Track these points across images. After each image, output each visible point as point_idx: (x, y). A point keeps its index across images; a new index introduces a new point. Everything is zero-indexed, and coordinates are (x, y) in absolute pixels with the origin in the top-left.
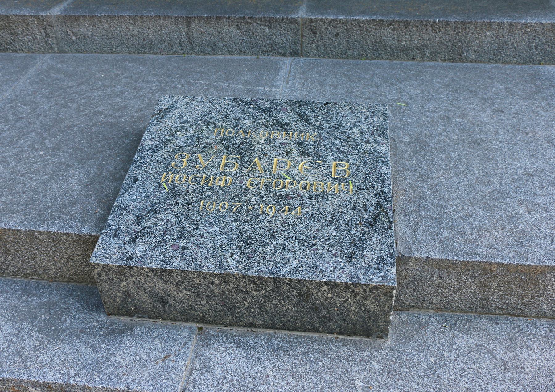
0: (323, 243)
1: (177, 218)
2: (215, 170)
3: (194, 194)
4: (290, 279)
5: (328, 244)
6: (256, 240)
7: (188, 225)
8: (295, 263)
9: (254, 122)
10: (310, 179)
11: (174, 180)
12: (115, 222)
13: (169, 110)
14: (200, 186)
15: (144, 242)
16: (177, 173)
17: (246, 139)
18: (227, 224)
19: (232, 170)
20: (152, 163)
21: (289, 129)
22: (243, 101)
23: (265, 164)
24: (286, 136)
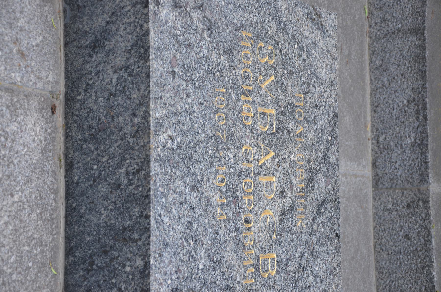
0: (190, 253)
1: (204, 59)
3: (231, 77)
4: (150, 216)
5: (189, 259)
6: (188, 166)
7: (198, 75)
8: (167, 220)
9: (313, 144)
10: (256, 227)
13: (321, 27)
14: (241, 84)
17: (294, 136)
18: (202, 126)
19: (259, 123)
20: (262, 14)
21: (307, 191)
22: (335, 126)
23: (269, 166)
24: (299, 188)
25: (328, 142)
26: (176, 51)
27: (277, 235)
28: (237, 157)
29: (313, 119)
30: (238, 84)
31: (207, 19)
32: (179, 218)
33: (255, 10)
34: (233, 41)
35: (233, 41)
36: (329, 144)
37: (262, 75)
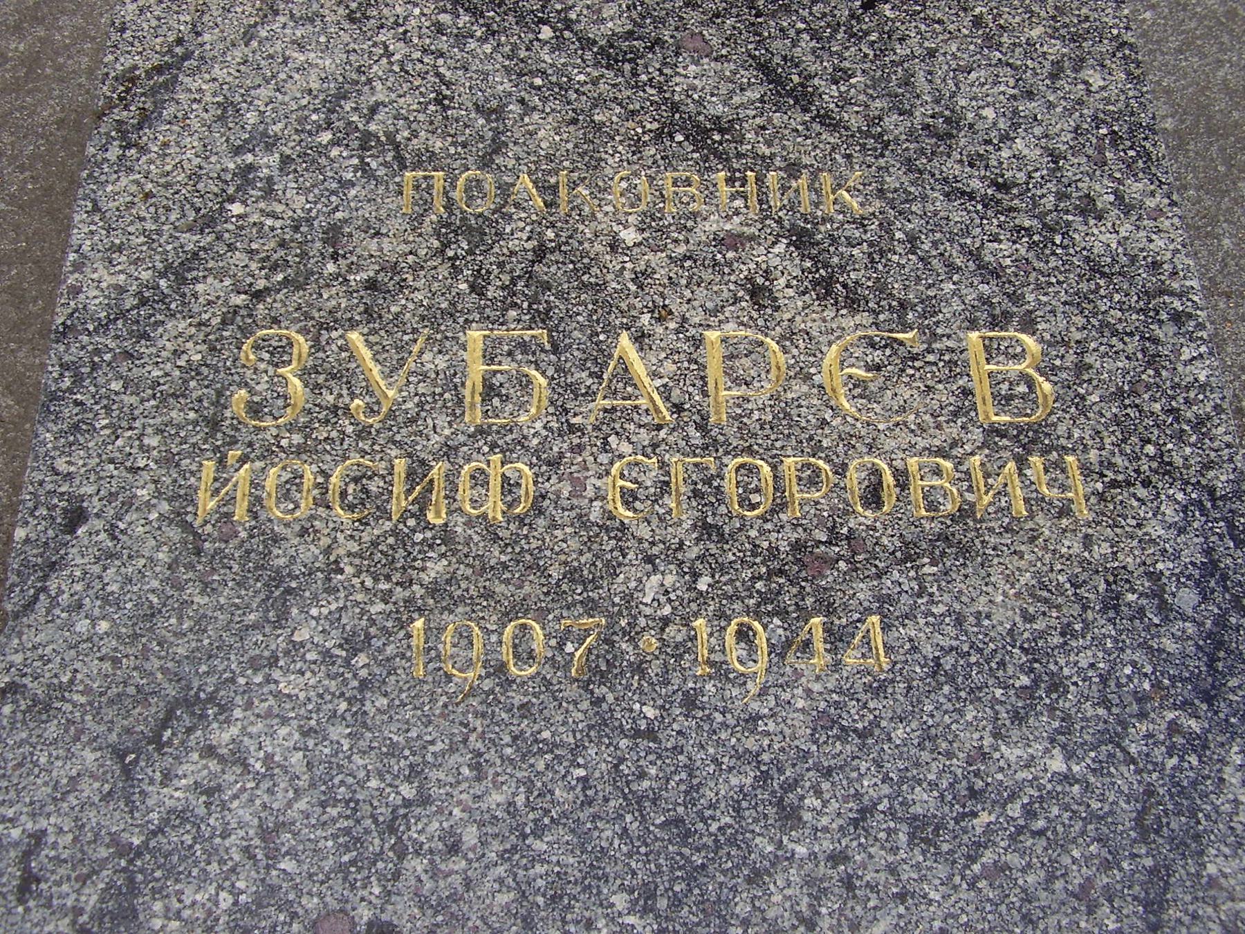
1: (311, 743)
2: (442, 420)
3: (369, 583)
5: (1041, 833)
6: (710, 843)
7: (374, 783)
9: (574, 121)
10: (890, 444)
11: (259, 500)
12: (13, 794)
15: (178, 915)
16: (268, 453)
20: (133, 400)
21: (739, 156)
24: (733, 197)
25: (558, 44)
26: (294, 915)
27: (906, 327)
28: (655, 550)
29: (488, 121)
30: (391, 540)
31: (164, 725)
32: (902, 897)
33: (119, 442)
34: (236, 568)
35: (236, 568)
36: (567, 34)
37: (347, 400)
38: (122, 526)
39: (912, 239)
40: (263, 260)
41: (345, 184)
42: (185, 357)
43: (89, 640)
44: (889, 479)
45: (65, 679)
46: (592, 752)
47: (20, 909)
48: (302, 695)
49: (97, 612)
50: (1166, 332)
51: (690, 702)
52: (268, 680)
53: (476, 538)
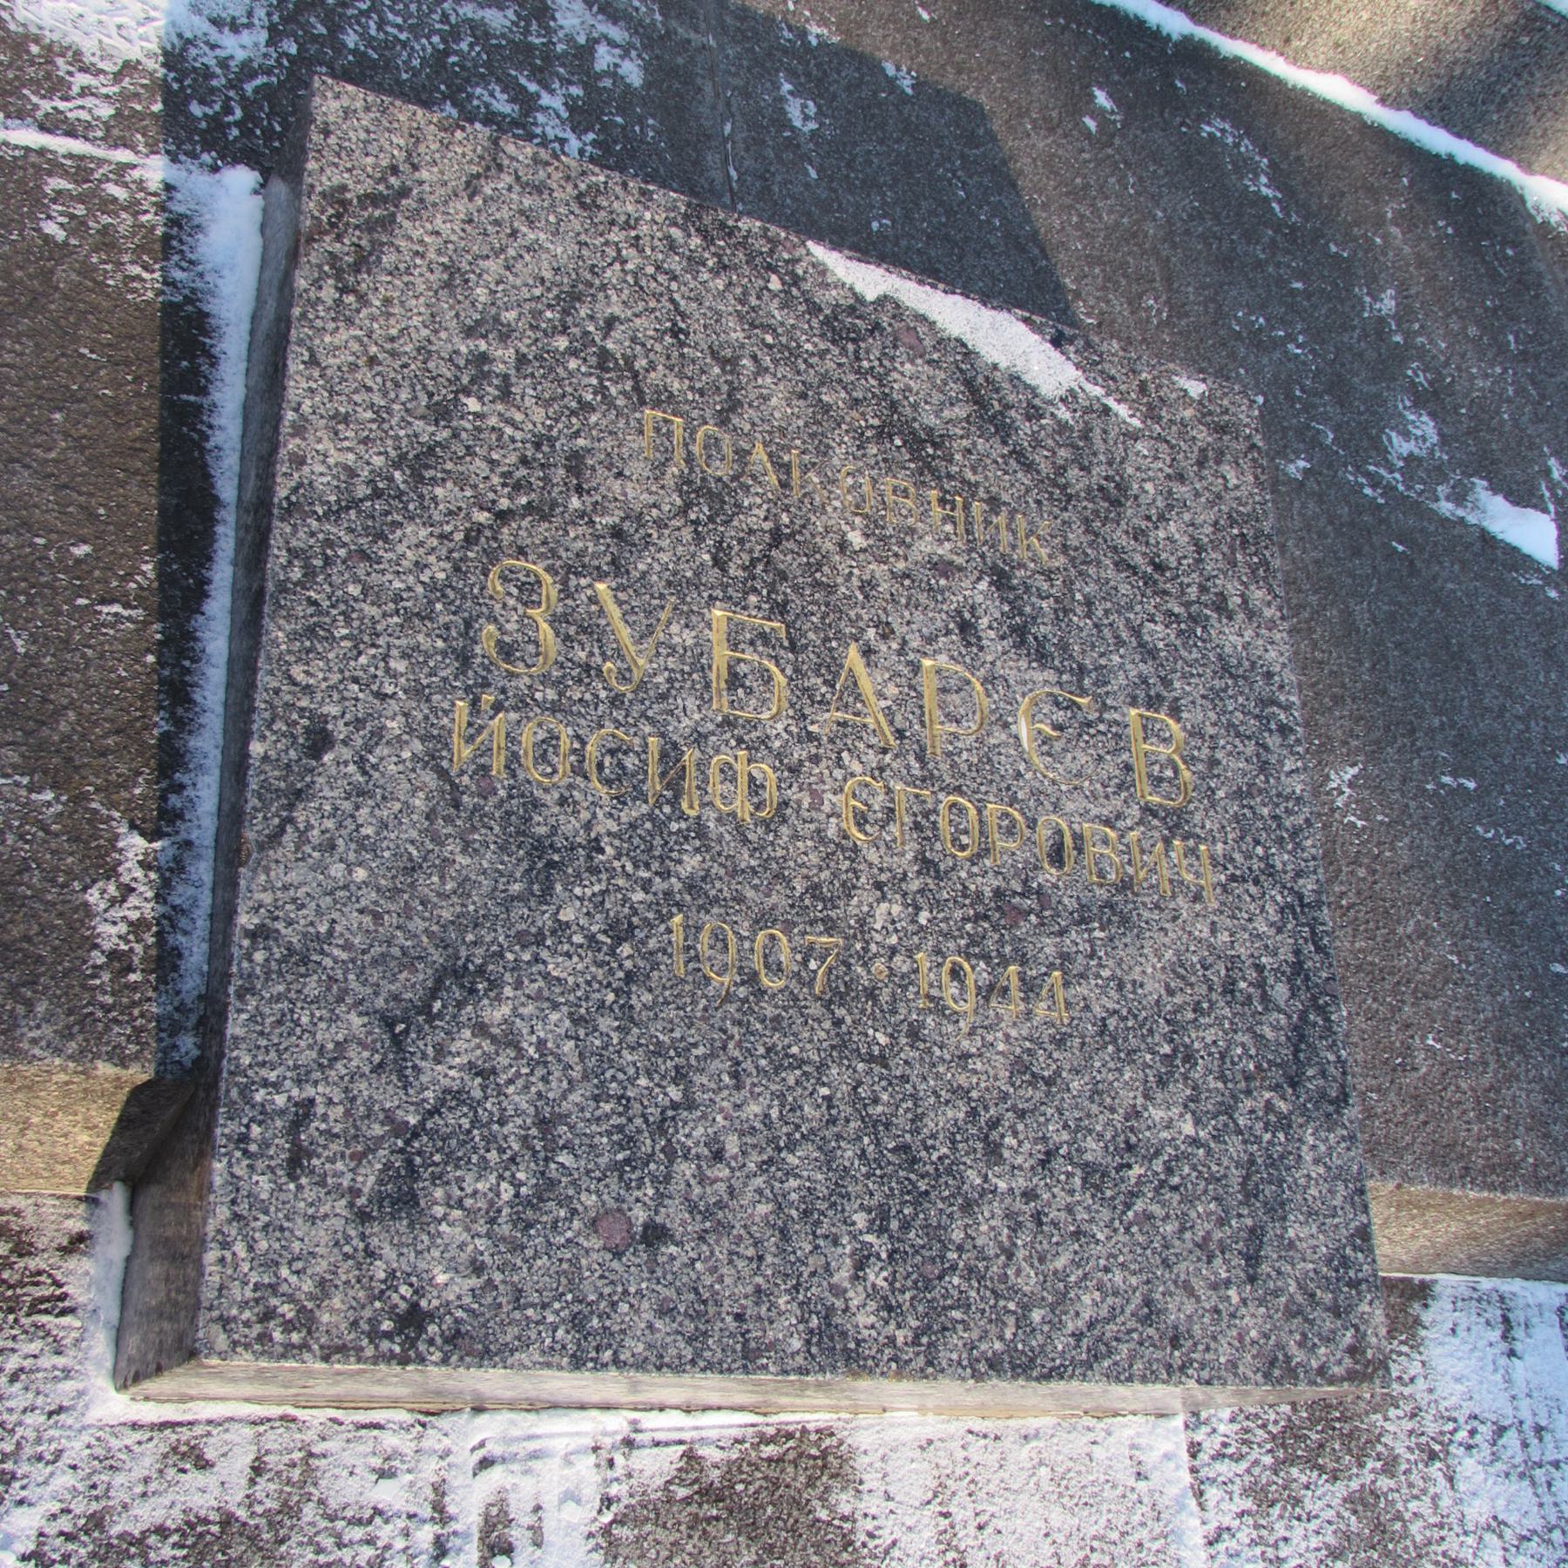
2: (691, 703)
3: (629, 868)
5: (1175, 1188)
7: (643, 1082)
9: (803, 396)
11: (515, 755)
12: (273, 1055)
15: (460, 1204)
20: (374, 611)
21: (950, 477)
26: (574, 1212)
27: (1083, 692)
28: (883, 877)
30: (648, 825)
31: (434, 994)
32: (1077, 1234)
33: (363, 660)
35: (497, 829)
36: (795, 291)
37: (599, 660)
38: (373, 760)
39: (1089, 603)
40: (504, 475)
41: (586, 407)
42: (428, 573)
43: (345, 887)
44: (1068, 841)
45: (323, 929)
46: (834, 1071)
47: (292, 1186)
48: (571, 980)
49: (352, 856)
50: (1273, 741)
51: (914, 1034)
52: (537, 959)
53: (728, 837)
